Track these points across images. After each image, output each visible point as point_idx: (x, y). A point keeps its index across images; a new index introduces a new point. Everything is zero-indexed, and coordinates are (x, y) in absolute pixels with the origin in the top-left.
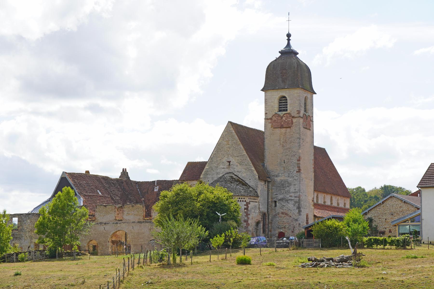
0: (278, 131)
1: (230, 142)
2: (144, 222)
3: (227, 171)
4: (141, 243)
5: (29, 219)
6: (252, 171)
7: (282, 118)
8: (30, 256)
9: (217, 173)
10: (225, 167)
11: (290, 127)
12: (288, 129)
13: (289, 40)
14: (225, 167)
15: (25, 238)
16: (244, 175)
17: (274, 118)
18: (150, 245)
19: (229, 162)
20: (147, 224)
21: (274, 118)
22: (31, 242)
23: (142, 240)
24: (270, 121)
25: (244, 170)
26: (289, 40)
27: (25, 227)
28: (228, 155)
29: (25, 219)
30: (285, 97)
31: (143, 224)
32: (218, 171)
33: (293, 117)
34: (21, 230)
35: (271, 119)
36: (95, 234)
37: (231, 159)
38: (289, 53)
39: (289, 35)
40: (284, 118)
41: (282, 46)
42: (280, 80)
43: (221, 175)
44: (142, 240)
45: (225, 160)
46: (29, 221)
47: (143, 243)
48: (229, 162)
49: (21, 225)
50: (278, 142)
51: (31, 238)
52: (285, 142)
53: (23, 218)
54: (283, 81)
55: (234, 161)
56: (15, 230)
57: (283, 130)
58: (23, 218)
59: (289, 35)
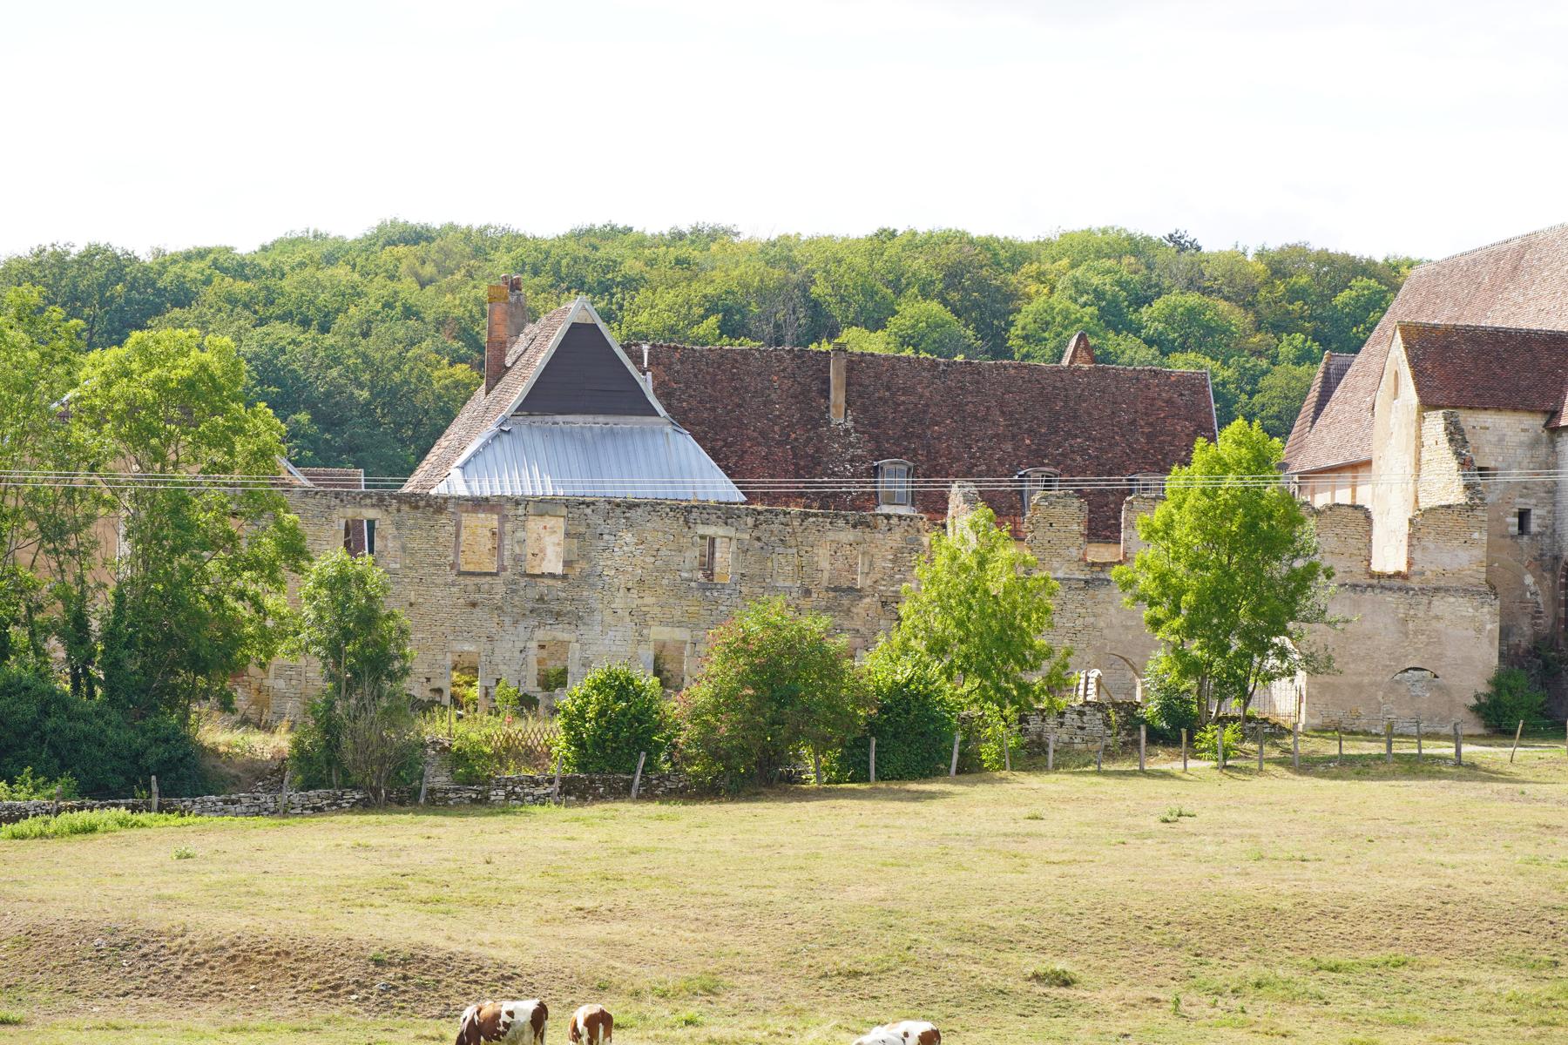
2: (1370, 586)
4: (1356, 679)
5: (630, 525)
8: (1064, 730)
15: (609, 618)
18: (1402, 689)
20: (1390, 598)
22: (642, 639)
23: (1363, 667)
27: (606, 564)
29: (604, 528)
31: (1369, 594)
34: (585, 577)
36: (1127, 628)
44: (1363, 667)
46: (628, 537)
47: (1366, 680)
49: (584, 556)
51: (641, 619)
53: (596, 519)
56: (552, 576)
58: (596, 519)
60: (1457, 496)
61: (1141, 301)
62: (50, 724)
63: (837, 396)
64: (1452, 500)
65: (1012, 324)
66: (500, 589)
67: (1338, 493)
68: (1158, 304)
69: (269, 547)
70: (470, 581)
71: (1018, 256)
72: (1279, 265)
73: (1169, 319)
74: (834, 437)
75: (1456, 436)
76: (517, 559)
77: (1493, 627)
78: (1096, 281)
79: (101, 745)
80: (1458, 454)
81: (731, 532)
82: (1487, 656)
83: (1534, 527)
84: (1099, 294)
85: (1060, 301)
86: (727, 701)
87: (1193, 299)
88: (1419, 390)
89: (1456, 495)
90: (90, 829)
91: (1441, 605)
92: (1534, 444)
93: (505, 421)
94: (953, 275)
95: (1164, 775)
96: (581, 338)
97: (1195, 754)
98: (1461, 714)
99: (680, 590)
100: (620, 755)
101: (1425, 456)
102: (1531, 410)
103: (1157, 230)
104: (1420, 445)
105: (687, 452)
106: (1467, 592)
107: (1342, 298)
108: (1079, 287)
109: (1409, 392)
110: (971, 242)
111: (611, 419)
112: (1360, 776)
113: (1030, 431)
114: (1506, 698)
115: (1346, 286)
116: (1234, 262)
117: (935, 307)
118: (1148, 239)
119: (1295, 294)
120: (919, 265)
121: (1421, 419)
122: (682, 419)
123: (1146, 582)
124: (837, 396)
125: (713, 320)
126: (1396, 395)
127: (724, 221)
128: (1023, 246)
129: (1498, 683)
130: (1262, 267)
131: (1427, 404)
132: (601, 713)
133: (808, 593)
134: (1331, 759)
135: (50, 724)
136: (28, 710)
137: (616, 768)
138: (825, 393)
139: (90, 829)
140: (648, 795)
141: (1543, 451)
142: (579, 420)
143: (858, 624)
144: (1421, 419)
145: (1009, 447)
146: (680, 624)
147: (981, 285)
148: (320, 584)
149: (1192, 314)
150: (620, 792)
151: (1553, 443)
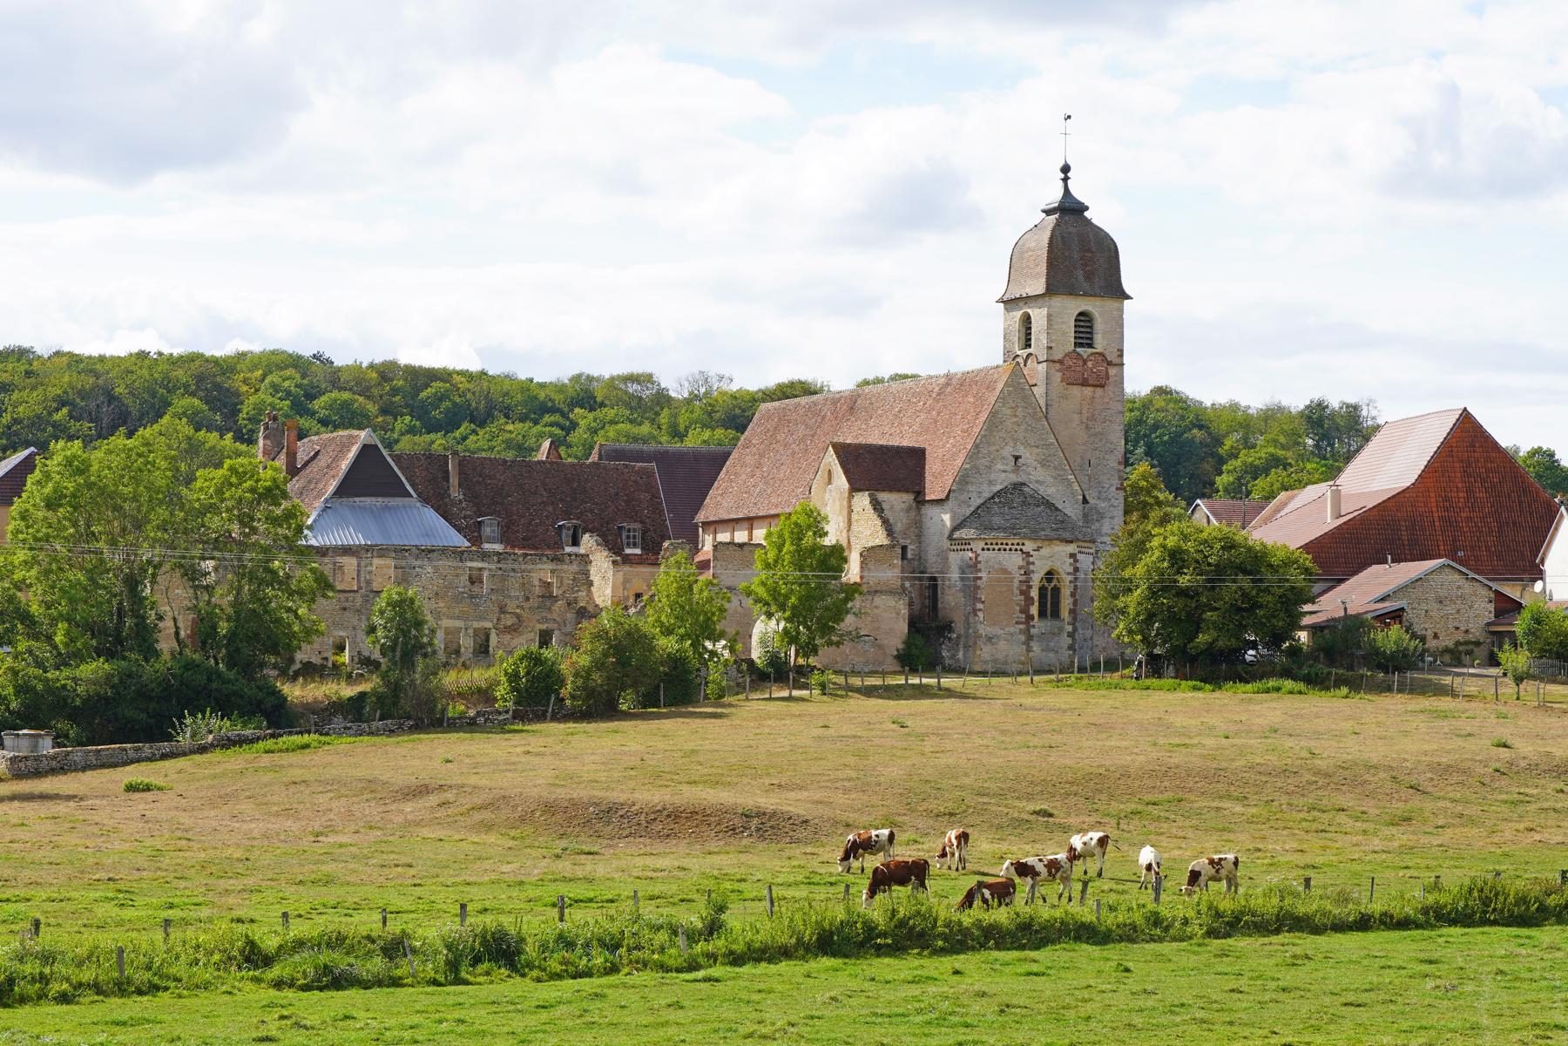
0: (1076, 391)
1: (1020, 412)
3: (1013, 478)
6: (1070, 484)
7: (1085, 362)
9: (991, 483)
10: (1009, 468)
11: (1102, 386)
12: (1099, 391)
13: (1065, 180)
14: (1009, 468)
16: (1051, 490)
17: (1068, 362)
19: (1017, 458)
21: (1068, 362)
24: (1058, 366)
25: (1050, 479)
26: (1065, 180)
28: (1015, 441)
30: (1081, 314)
32: (993, 477)
33: (1110, 364)
35: (1061, 362)
37: (1021, 451)
38: (1070, 210)
39: (1066, 169)
40: (1090, 364)
41: (1054, 196)
42: (1080, 273)
43: (999, 487)
45: (1008, 451)
48: (1017, 458)
50: (1076, 417)
52: (1092, 418)
54: (1089, 277)
55: (1028, 456)
57: (1088, 391)
59: (1066, 169)
60: (886, 542)
61: (311, 397)
62: (214, 685)
63: (454, 480)
64: (878, 542)
65: (240, 411)
66: (359, 600)
67: (737, 534)
68: (324, 398)
69: (309, 582)
70: (342, 596)
71: (227, 366)
72: (386, 371)
73: (330, 407)
74: (454, 504)
75: (877, 506)
76: (368, 582)
77: (905, 612)
78: (286, 384)
79: (242, 697)
80: (880, 516)
81: (485, 565)
82: (903, 627)
83: (909, 556)
84: (288, 393)
85: (264, 396)
86: (598, 665)
87: (346, 395)
88: (849, 480)
89: (881, 538)
90: (306, 746)
91: (878, 600)
92: (909, 510)
93: (326, 501)
94: (200, 379)
95: (802, 699)
96: (367, 449)
97: (805, 686)
98: (890, 660)
99: (458, 599)
100: (538, 698)
101: (854, 517)
102: (907, 491)
103: (307, 352)
104: (850, 511)
105: (431, 516)
106: (891, 592)
107: (423, 395)
108: (275, 388)
109: (841, 481)
110: (207, 360)
111: (386, 500)
112: (899, 697)
113: (561, 500)
114: (915, 651)
115: (427, 386)
116: (357, 368)
117: (196, 402)
118: (300, 357)
119: (395, 391)
120: (180, 374)
121: (851, 497)
122: (425, 500)
123: (762, 592)
124: (454, 480)
125: (65, 410)
126: (830, 482)
127: (26, 345)
128: (215, 361)
129: (908, 643)
130: (374, 375)
131: (855, 488)
132: (528, 673)
133: (527, 599)
134: (880, 687)
135: (214, 685)
136: (201, 679)
137: (537, 704)
138: (446, 477)
139: (306, 746)
140: (554, 718)
141: (913, 514)
142: (368, 501)
143: (555, 616)
144: (851, 497)
145: (550, 509)
146: (458, 618)
147: (218, 387)
148: (388, 604)
149: (346, 405)
150: (541, 717)
151: (918, 509)
